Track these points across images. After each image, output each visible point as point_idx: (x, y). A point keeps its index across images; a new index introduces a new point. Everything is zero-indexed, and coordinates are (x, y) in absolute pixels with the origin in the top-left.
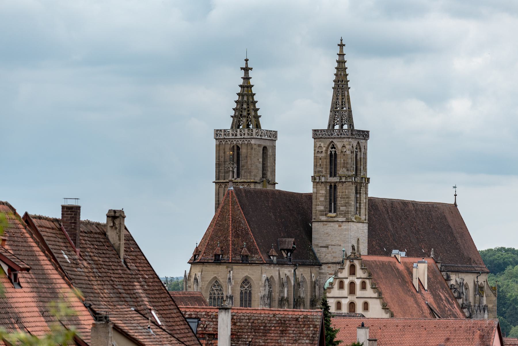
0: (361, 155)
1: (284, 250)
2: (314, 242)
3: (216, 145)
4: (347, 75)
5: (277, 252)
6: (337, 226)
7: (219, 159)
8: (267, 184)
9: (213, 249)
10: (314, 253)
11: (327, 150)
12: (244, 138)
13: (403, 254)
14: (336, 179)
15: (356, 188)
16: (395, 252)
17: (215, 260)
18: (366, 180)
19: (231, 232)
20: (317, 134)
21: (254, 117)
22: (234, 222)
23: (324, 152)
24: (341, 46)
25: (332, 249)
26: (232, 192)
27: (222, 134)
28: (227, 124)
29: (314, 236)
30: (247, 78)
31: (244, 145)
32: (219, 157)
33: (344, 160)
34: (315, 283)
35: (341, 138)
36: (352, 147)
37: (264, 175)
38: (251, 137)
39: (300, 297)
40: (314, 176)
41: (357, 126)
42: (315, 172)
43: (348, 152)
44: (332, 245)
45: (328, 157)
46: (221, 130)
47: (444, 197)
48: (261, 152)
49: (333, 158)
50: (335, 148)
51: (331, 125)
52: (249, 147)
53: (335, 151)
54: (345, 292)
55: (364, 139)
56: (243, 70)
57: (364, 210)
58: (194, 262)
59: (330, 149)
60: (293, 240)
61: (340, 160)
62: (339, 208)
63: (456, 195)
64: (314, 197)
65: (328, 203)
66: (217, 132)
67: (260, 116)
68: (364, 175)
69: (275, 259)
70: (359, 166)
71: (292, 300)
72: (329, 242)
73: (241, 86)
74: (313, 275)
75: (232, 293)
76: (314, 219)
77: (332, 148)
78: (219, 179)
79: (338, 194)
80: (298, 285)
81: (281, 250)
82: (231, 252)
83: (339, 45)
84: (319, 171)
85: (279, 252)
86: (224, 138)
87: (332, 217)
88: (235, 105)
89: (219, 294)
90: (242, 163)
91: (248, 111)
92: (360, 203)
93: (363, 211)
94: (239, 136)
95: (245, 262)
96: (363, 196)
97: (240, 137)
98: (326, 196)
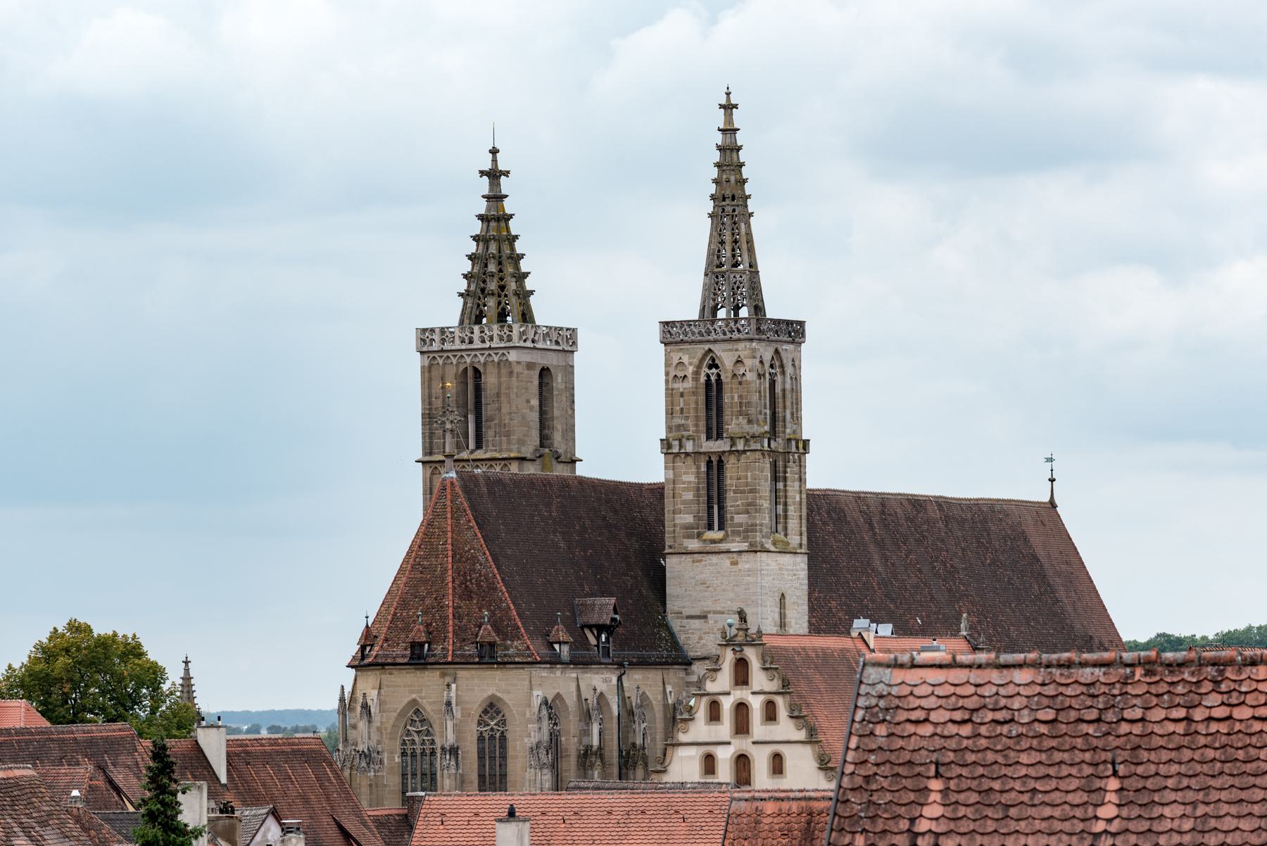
0: (784, 382)
1: (590, 627)
2: (671, 605)
3: (423, 368)
4: (745, 181)
5: (570, 631)
6: (728, 562)
7: (430, 404)
8: (554, 462)
9: (407, 629)
10: (672, 635)
12: (490, 348)
13: (886, 629)
14: (721, 446)
15: (774, 465)
16: (860, 623)
17: (411, 658)
18: (801, 445)
19: (450, 585)
20: (672, 334)
21: (516, 294)
22: (459, 561)
23: (690, 376)
24: (729, 108)
25: (716, 622)
26: (452, 483)
27: (437, 337)
28: (449, 313)
29: (671, 589)
30: (496, 198)
31: (490, 365)
32: (430, 397)
33: (740, 397)
34: (675, 709)
35: (731, 340)
36: (761, 362)
37: (544, 440)
38: (507, 344)
39: (634, 745)
40: (667, 439)
41: (772, 312)
42: (669, 429)
43: (751, 376)
44: (715, 612)
45: (702, 391)
46: (432, 330)
48: (536, 382)
49: (713, 392)
50: (717, 367)
51: (708, 310)
52: (504, 371)
53: (719, 375)
54: (724, 729)
55: (793, 342)
56: (485, 178)
57: (796, 521)
58: (361, 664)
59: (705, 370)
60: (613, 600)
61: (730, 397)
62: (732, 518)
64: (668, 492)
65: (704, 506)
66: (425, 336)
67: (532, 292)
68: (794, 432)
69: (565, 651)
70: (779, 410)
71: (616, 754)
72: (708, 605)
73: (481, 217)
74: (669, 688)
75: (458, 739)
76: (670, 547)
77: (710, 367)
78: (431, 454)
79: (728, 482)
80: (628, 713)
81: (583, 627)
82: (451, 635)
83: (721, 106)
84: (679, 427)
85: (578, 633)
86: (442, 351)
87: (713, 541)
88: (467, 266)
89: (423, 743)
90: (487, 411)
91: (501, 279)
92: (786, 504)
93: (793, 524)
94: (477, 344)
95: (487, 659)
96: (793, 487)
97: (481, 346)
98: (698, 489)
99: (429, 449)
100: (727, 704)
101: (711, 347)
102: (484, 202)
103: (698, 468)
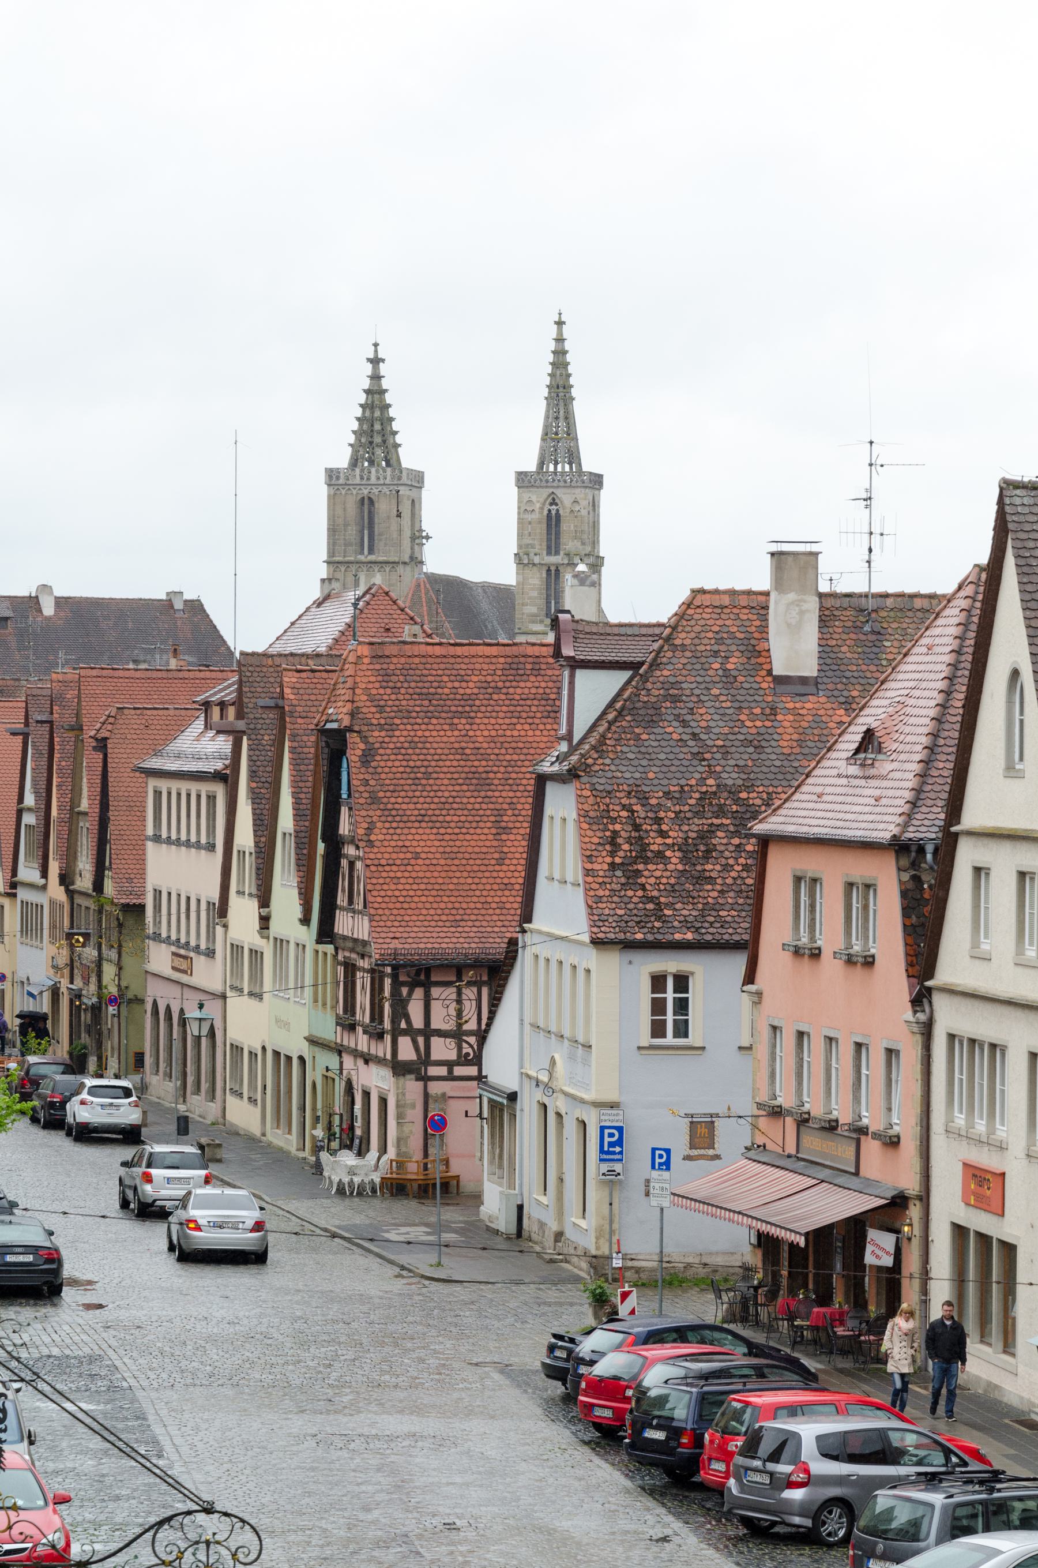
3: (329, 496)
7: (334, 521)
11: (542, 508)
12: (384, 484)
14: (553, 559)
20: (523, 480)
23: (537, 510)
24: (560, 323)
28: (342, 459)
30: (376, 377)
32: (334, 516)
33: (576, 526)
42: (520, 547)
50: (557, 505)
53: (558, 510)
66: (332, 475)
77: (551, 504)
99: (331, 552)
101: (557, 492)
102: (368, 380)
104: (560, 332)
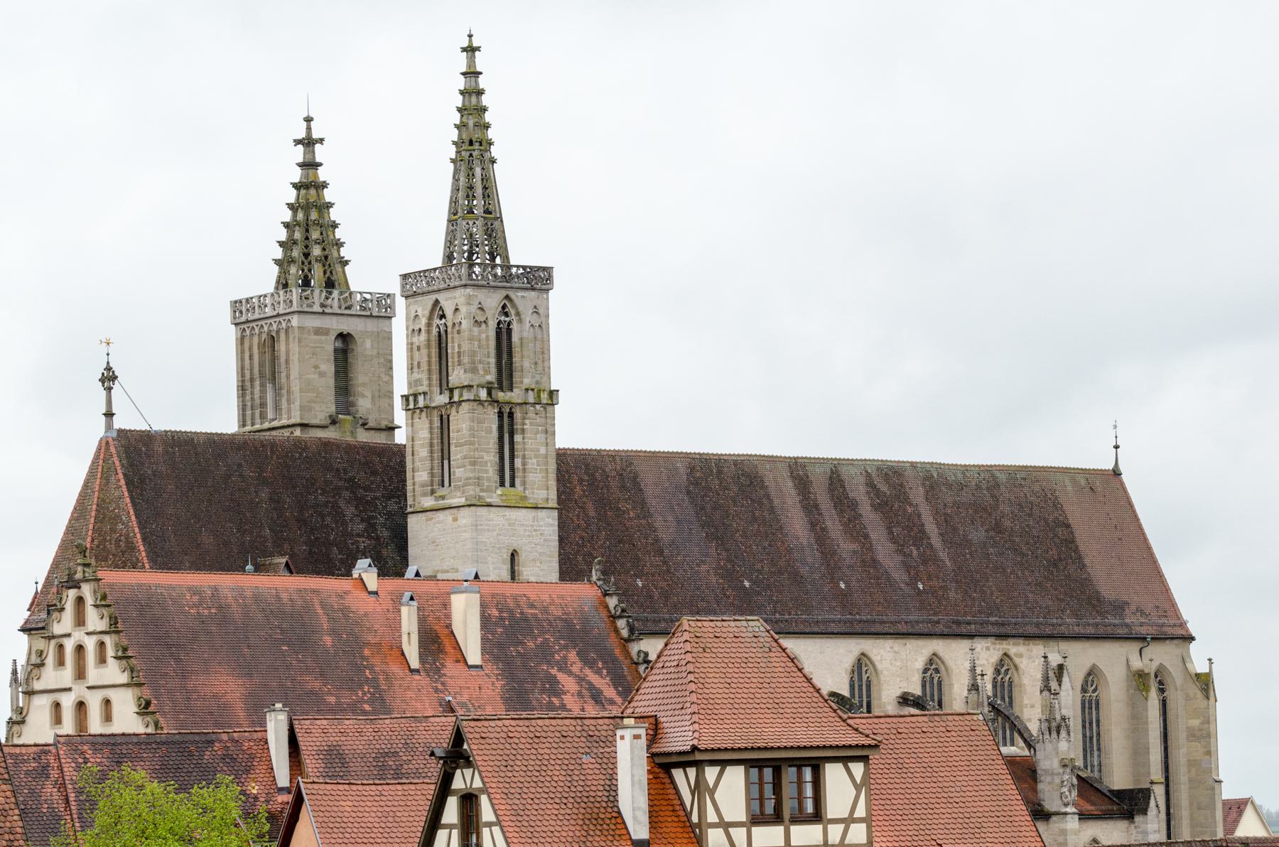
6: (450, 518)
11: (429, 325)
24: (471, 50)
29: (412, 550)
30: (310, 165)
33: (459, 346)
42: (410, 385)
45: (434, 344)
47: (1091, 455)
56: (300, 147)
61: (452, 349)
63: (1117, 447)
64: (409, 451)
65: (437, 462)
73: (295, 186)
92: (524, 457)
98: (431, 445)
100: (69, 646)
103: (431, 423)
104: (471, 61)
